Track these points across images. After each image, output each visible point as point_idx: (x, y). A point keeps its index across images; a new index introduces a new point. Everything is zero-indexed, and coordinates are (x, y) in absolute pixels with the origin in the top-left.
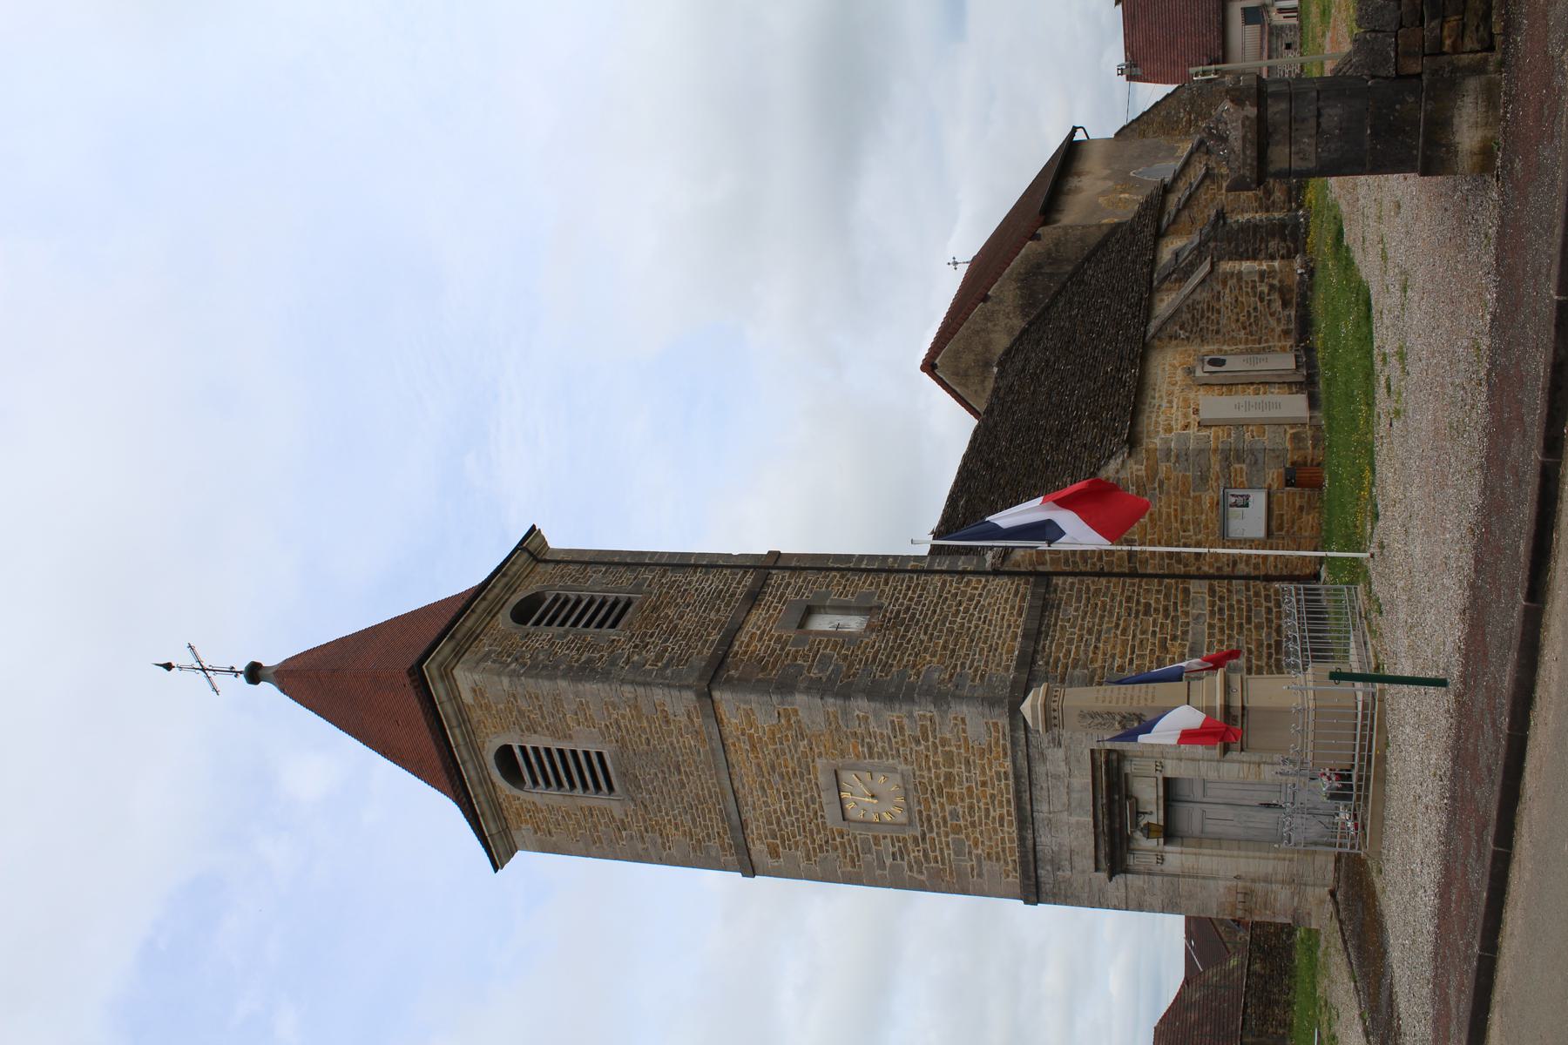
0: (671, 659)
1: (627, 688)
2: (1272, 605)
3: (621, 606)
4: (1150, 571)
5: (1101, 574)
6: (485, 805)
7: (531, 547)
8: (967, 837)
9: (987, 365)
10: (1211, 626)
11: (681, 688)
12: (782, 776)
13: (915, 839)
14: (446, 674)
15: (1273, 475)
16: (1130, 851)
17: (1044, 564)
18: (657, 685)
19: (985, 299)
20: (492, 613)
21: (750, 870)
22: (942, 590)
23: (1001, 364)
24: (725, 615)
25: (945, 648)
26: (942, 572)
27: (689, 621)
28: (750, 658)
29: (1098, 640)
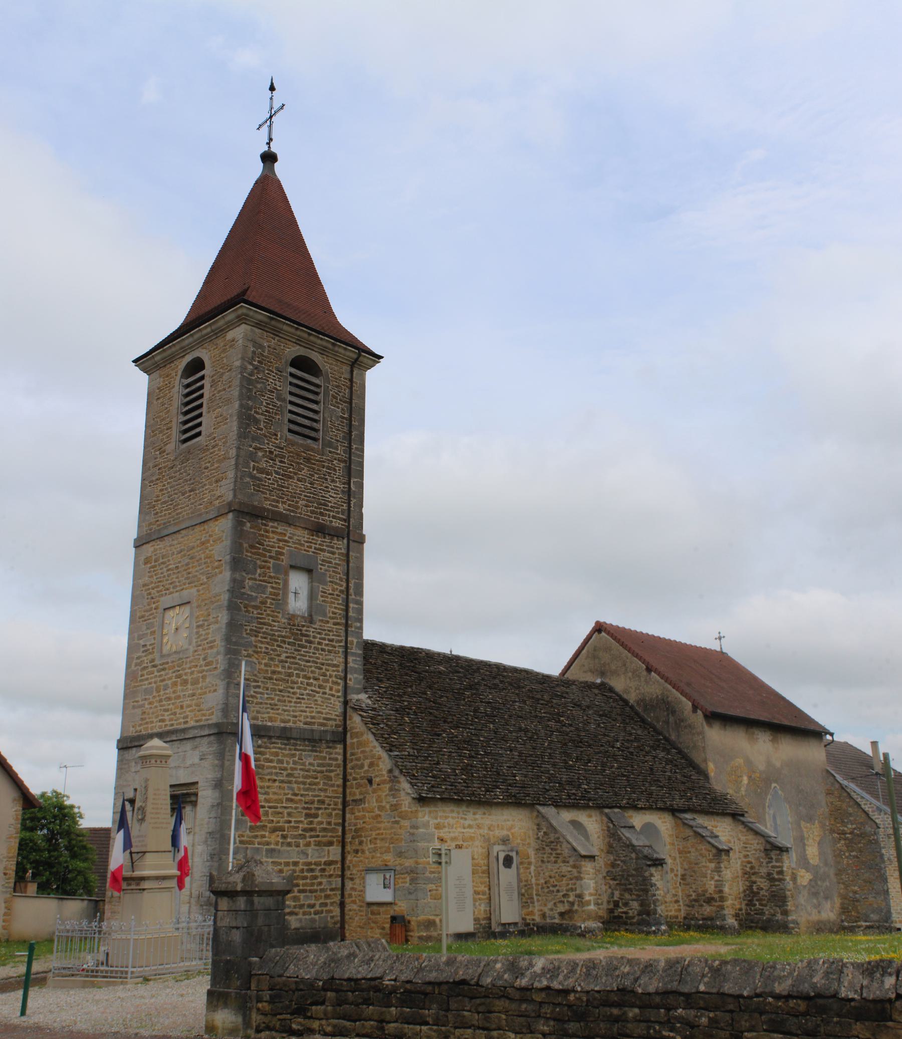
0: (260, 479)
1: (233, 452)
2: (317, 908)
3: (313, 434)
4: (348, 816)
5: (345, 780)
6: (169, 352)
7: (363, 357)
8: (154, 697)
9: (602, 674)
10: (296, 864)
11: (235, 490)
12: (187, 564)
13: (153, 661)
14: (242, 319)
15: (402, 907)
17: (352, 737)
18: (236, 473)
19: (649, 670)
20: (298, 342)
21: (139, 544)
22: (329, 665)
23: (603, 684)
24: (303, 511)
25: (274, 672)
26: (346, 663)
27: (294, 485)
28: (263, 535)
29: (282, 782)
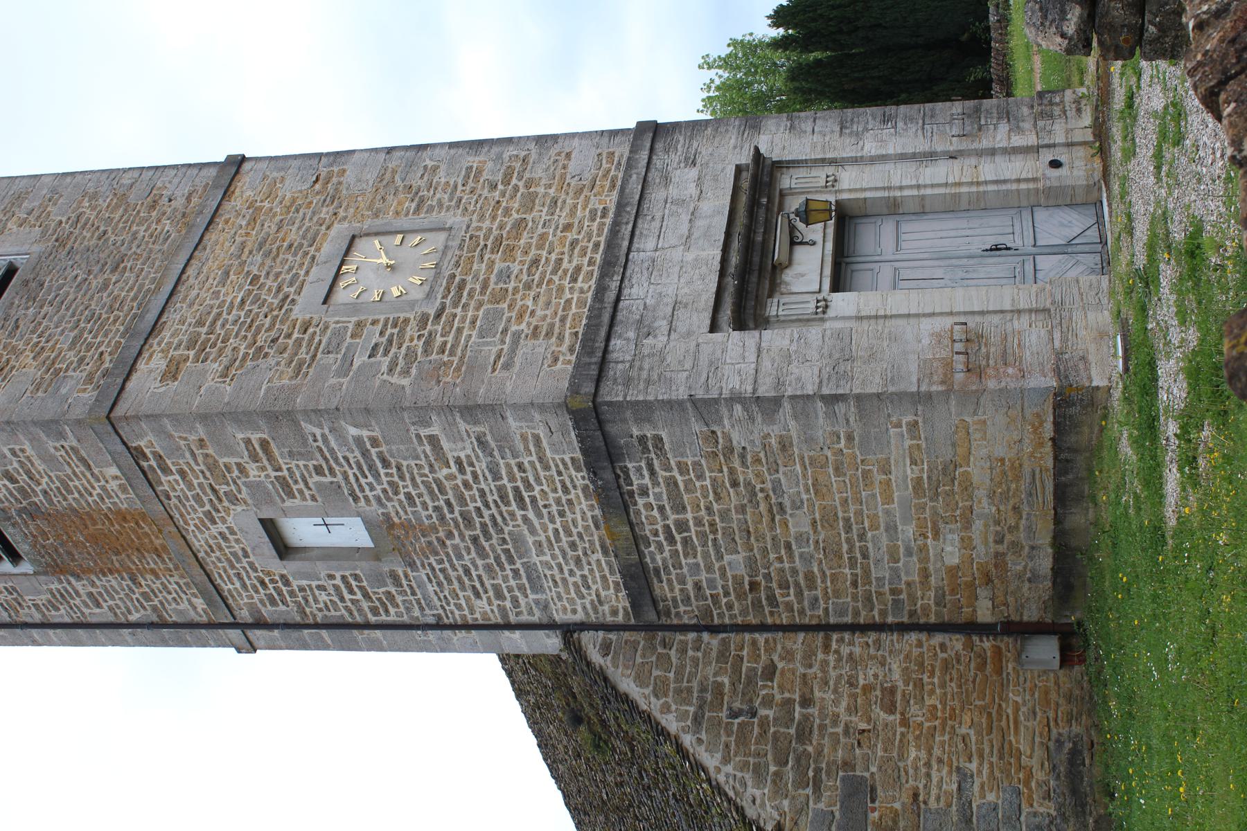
16: (773, 289)
